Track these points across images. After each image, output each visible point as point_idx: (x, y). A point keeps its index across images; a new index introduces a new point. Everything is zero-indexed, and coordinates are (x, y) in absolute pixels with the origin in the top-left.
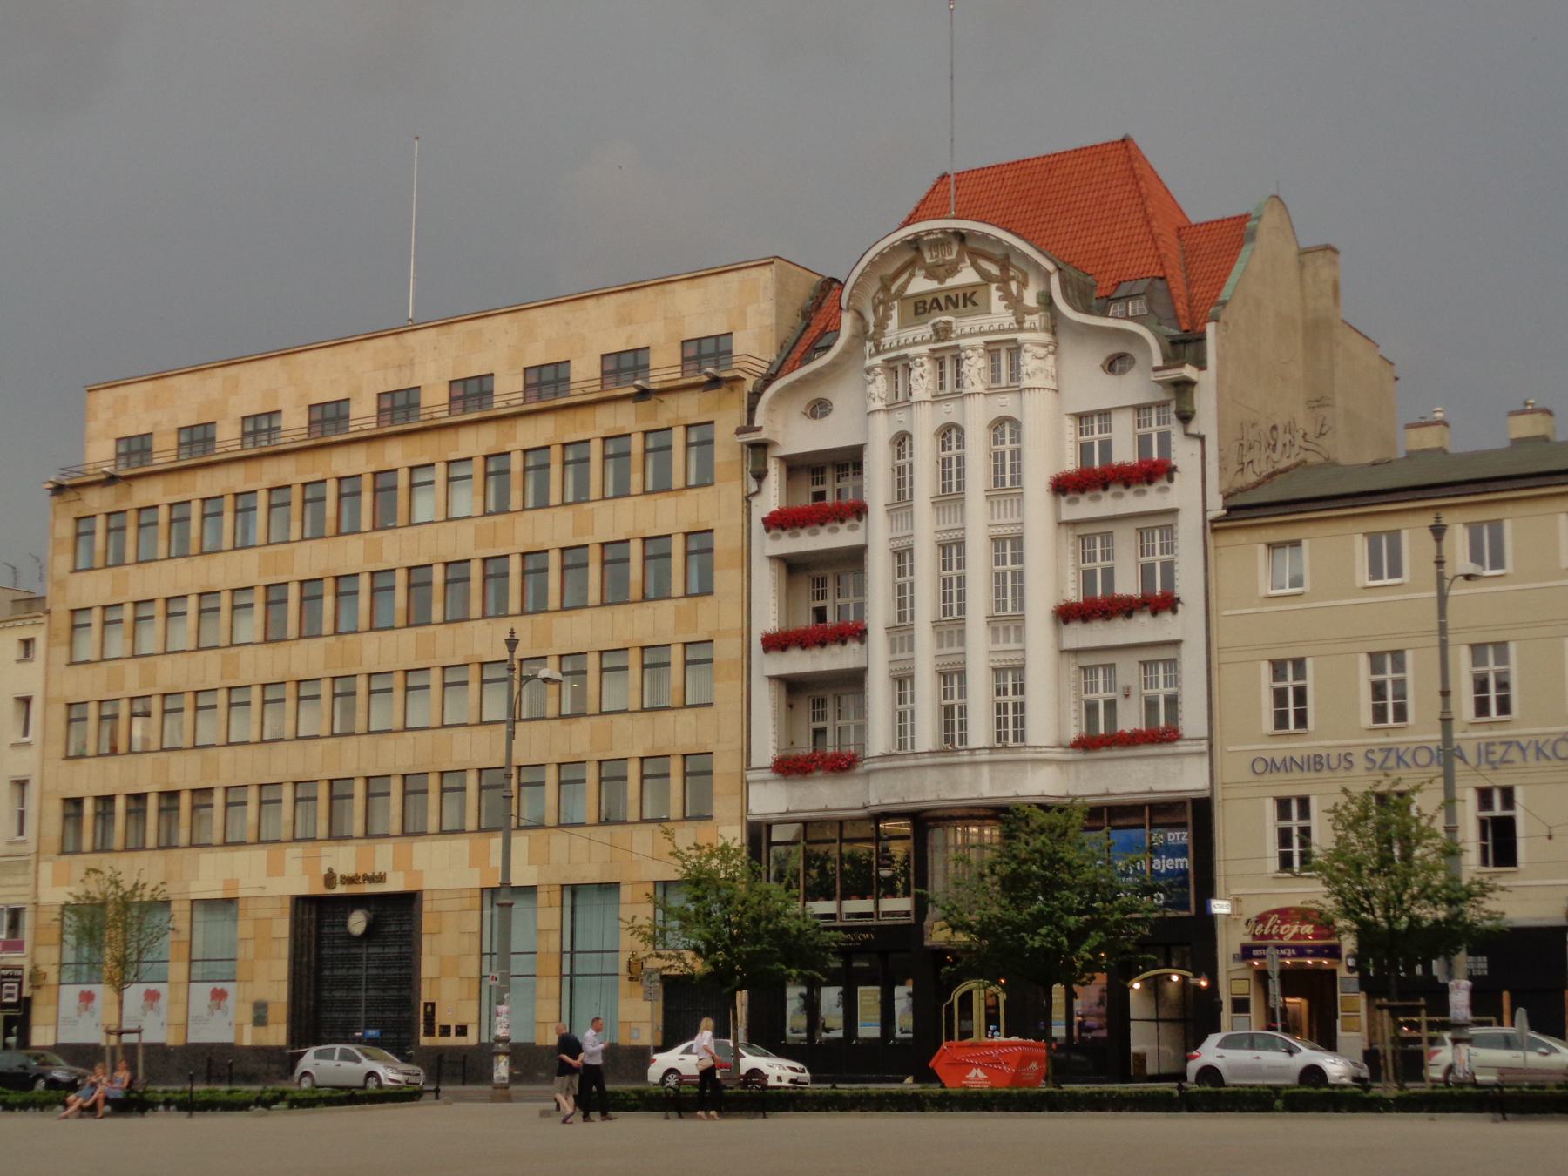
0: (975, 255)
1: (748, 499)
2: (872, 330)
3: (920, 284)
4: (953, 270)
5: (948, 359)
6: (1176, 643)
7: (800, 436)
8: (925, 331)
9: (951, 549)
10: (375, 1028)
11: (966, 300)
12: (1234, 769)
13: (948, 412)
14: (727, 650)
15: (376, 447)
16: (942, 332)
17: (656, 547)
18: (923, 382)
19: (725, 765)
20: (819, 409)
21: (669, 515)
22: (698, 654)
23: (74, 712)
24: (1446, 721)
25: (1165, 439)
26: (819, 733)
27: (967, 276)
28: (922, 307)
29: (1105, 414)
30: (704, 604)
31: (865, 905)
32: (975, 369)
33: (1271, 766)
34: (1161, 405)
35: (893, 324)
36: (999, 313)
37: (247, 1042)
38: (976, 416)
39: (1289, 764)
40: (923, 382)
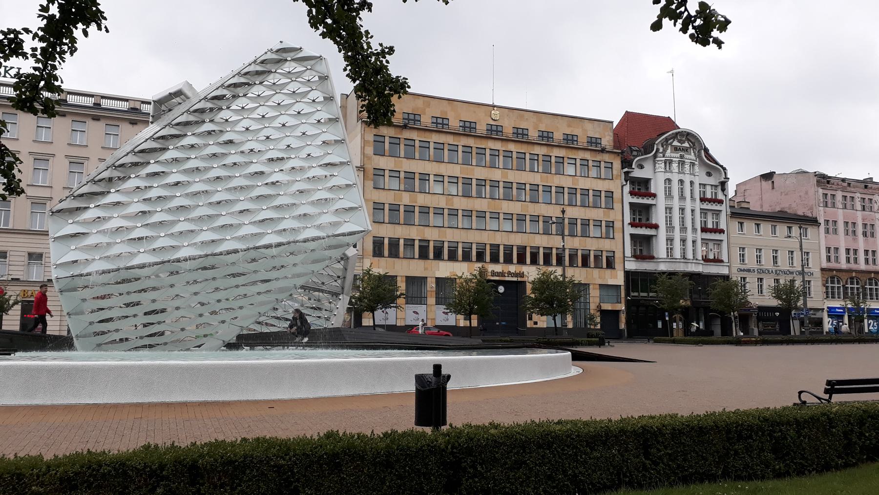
0: (689, 140)
1: (622, 187)
2: (661, 150)
3: (676, 143)
4: (684, 143)
5: (682, 163)
6: (721, 241)
7: (637, 173)
8: (678, 155)
9: (682, 210)
10: (575, 324)
11: (686, 150)
12: (734, 270)
13: (681, 177)
14: (618, 225)
15: (504, 143)
16: (682, 157)
17: (597, 193)
18: (675, 166)
19: (618, 255)
20: (641, 167)
21: (602, 186)
22: (610, 225)
23: (378, 207)
24: (803, 266)
25: (716, 193)
26: (641, 250)
27: (686, 145)
28: (676, 149)
29: (705, 185)
30: (611, 211)
31: (645, 294)
32: (687, 167)
33: (741, 270)
34: (716, 186)
35: (669, 151)
36: (692, 156)
37: (462, 325)
38: (687, 179)
39: (744, 270)
40: (675, 166)
